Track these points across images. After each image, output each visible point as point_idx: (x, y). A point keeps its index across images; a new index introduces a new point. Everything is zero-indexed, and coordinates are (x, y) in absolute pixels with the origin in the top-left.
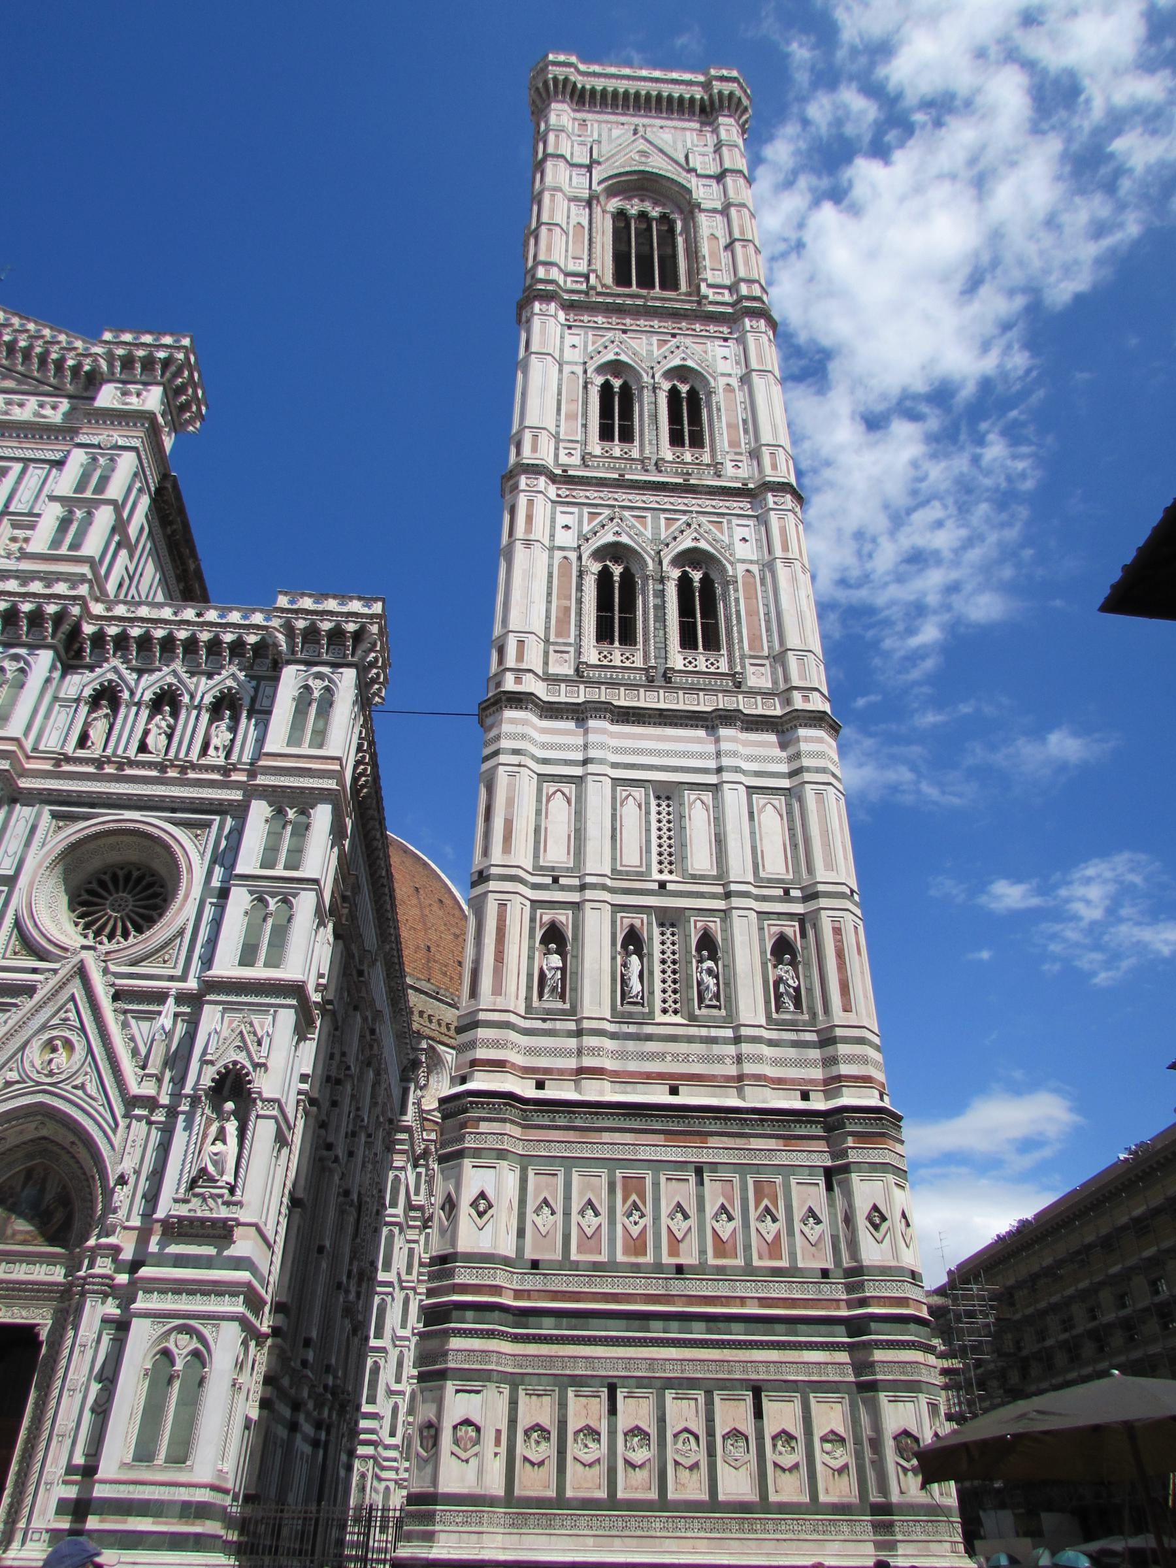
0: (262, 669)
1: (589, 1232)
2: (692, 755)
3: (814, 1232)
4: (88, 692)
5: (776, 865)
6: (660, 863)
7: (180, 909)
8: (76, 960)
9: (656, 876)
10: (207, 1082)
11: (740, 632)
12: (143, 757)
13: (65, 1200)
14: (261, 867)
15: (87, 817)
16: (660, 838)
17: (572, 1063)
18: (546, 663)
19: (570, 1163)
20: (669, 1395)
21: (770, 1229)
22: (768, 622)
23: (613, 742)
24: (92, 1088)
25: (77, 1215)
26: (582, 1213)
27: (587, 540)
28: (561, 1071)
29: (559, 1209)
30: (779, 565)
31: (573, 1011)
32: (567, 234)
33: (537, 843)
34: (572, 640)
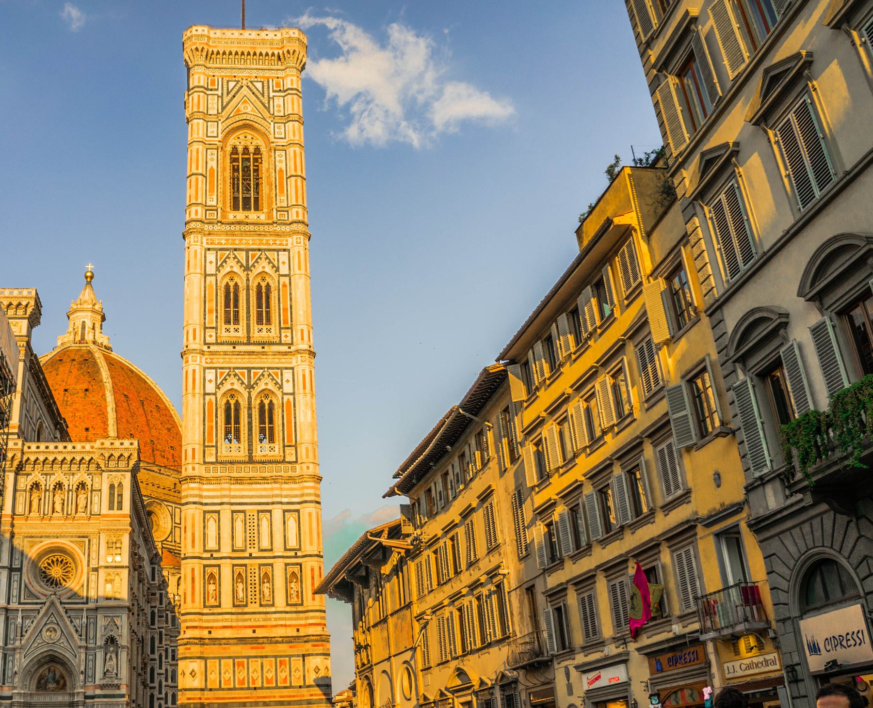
4: (29, 487)
5: (292, 543)
7: (80, 579)
8: (50, 599)
9: (249, 551)
10: (103, 643)
12: (55, 514)
13: (62, 677)
17: (220, 624)
19: (220, 658)
23: (233, 493)
24: (66, 644)
26: (225, 673)
27: (219, 388)
28: (217, 628)
31: (219, 606)
34: (214, 444)
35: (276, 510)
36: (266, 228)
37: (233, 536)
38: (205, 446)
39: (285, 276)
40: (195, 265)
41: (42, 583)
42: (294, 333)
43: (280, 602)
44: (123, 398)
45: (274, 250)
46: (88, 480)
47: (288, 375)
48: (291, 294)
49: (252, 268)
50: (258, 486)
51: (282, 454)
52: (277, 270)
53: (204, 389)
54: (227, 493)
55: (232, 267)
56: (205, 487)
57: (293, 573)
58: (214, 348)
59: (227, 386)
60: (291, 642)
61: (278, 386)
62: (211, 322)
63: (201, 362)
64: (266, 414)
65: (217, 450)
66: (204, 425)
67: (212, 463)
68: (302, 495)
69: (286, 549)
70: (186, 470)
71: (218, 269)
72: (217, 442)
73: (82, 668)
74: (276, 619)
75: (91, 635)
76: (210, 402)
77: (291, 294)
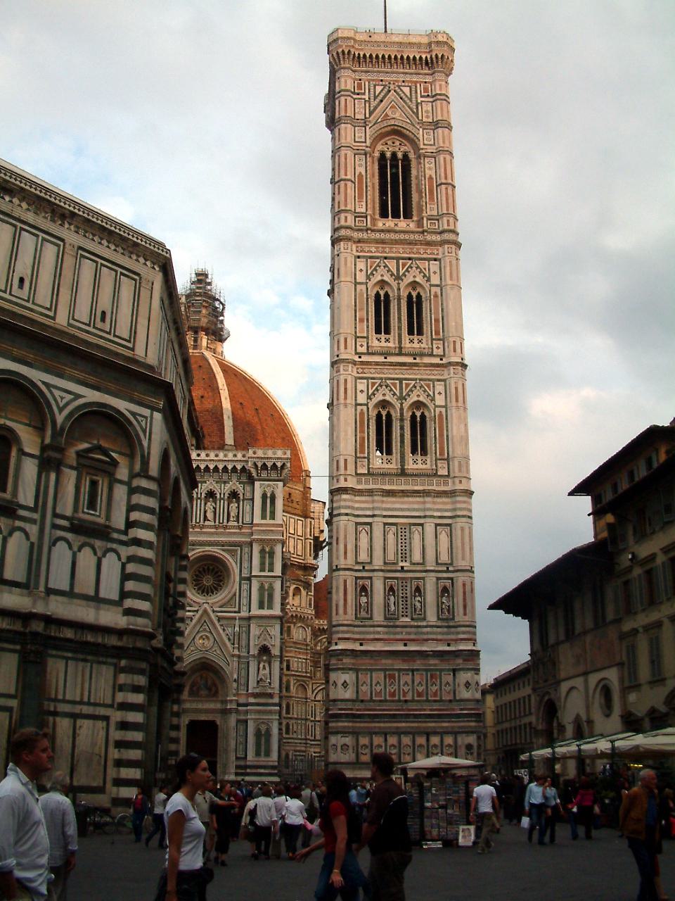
0: (244, 479)
1: (378, 691)
2: (414, 510)
3: (448, 688)
5: (444, 558)
6: (402, 557)
7: (232, 587)
8: (203, 608)
9: (401, 564)
11: (436, 446)
12: (207, 523)
13: (215, 685)
14: (261, 571)
15: (193, 550)
16: (402, 546)
17: (372, 636)
18: (356, 468)
20: (402, 736)
21: (434, 688)
22: (448, 440)
23: (384, 506)
25: (219, 689)
26: (376, 685)
27: (371, 399)
28: (368, 640)
29: (369, 684)
30: (454, 411)
31: (371, 618)
32: (355, 183)
33: (356, 552)
35: (428, 524)
36: (417, 237)
37: (384, 549)
38: (356, 457)
39: (437, 286)
40: (346, 273)
41: (194, 592)
42: (446, 344)
43: (432, 617)
44: (239, 406)
45: (425, 259)
46: (240, 488)
47: (440, 387)
48: (442, 304)
49: (403, 278)
50: (411, 499)
51: (434, 467)
52: (428, 280)
53: (356, 400)
54: (379, 505)
55: (382, 276)
56: (357, 498)
57: (445, 590)
58: (364, 358)
59: (379, 397)
60: (442, 656)
61: (430, 398)
62: (362, 331)
63: (352, 371)
64: (419, 427)
65: (369, 460)
66: (356, 435)
67: (364, 474)
68: (455, 510)
69: (437, 563)
70: (338, 482)
71: (368, 278)
72: (368, 453)
73: (235, 676)
74: (427, 633)
75: (244, 643)
76: (362, 413)
77: (442, 304)
